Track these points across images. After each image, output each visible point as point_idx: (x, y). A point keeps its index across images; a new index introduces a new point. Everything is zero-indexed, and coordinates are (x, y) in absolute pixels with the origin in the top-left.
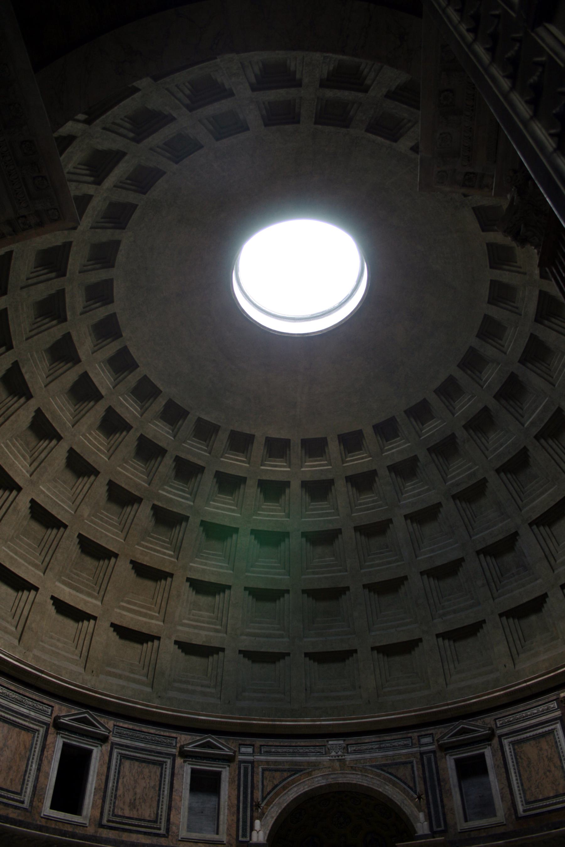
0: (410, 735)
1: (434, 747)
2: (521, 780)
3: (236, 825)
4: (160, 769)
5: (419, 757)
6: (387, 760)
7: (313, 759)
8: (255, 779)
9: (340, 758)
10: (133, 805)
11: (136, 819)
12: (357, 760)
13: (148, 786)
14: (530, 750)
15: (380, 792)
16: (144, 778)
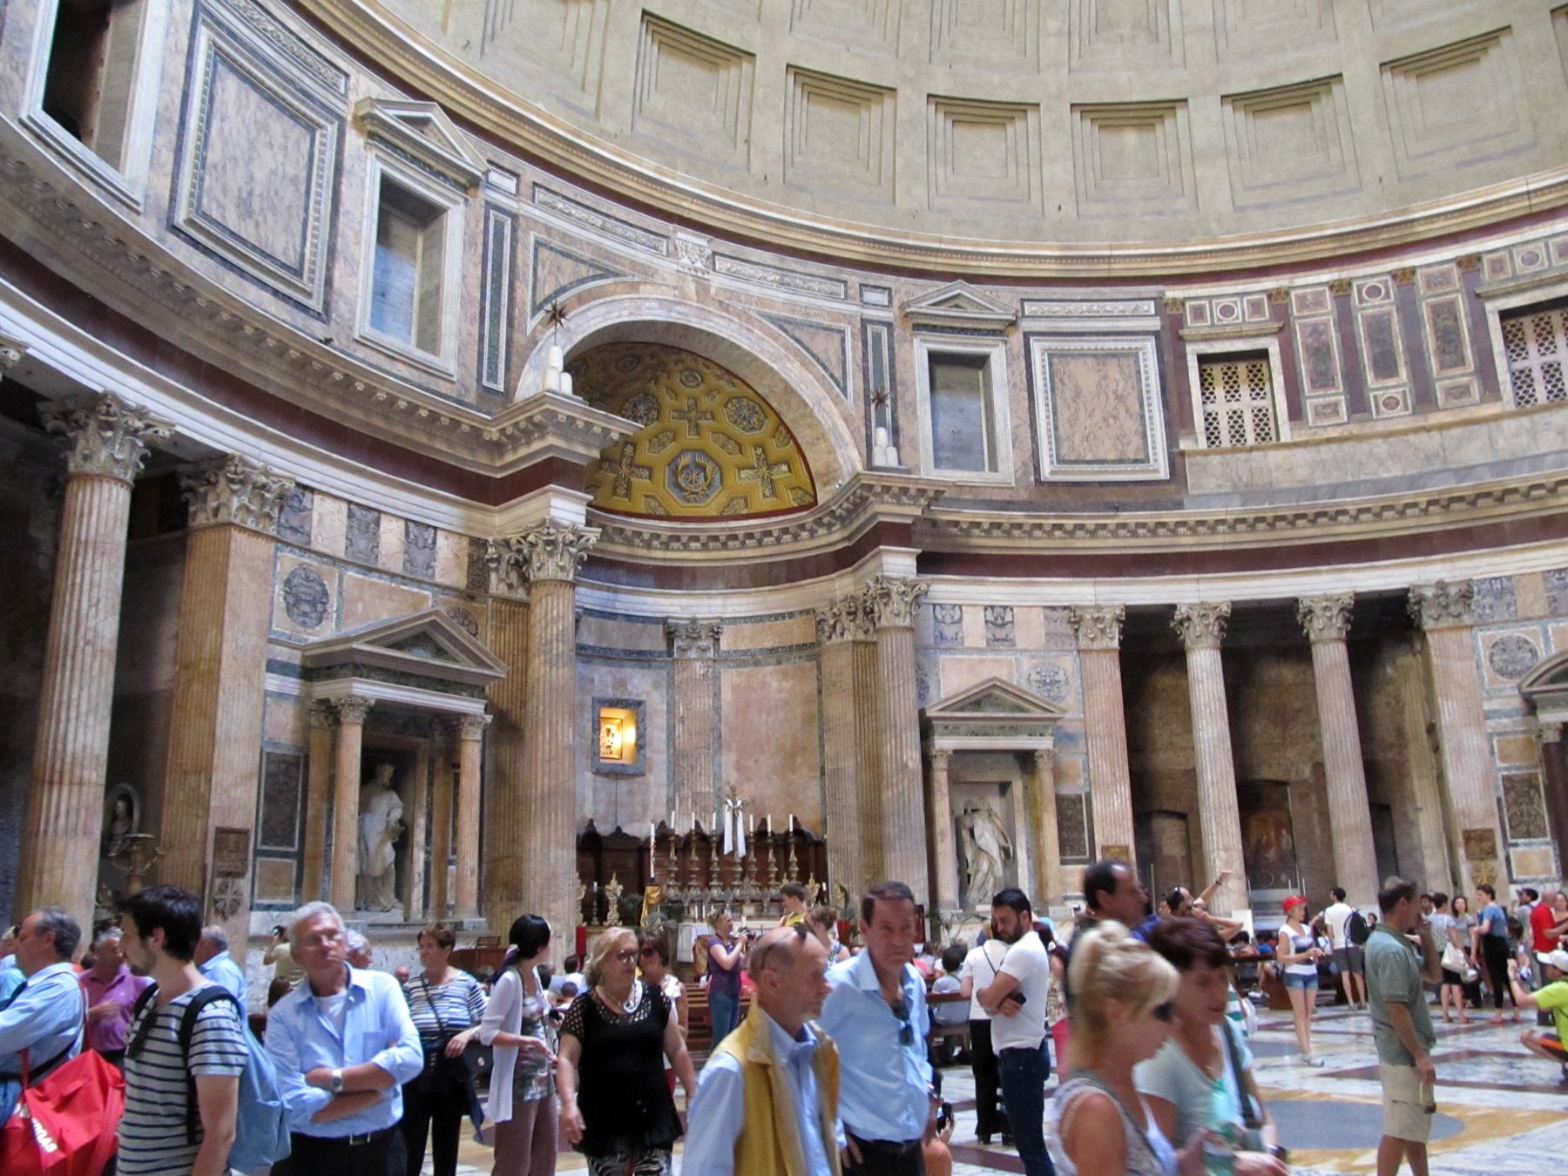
0: (844, 276)
1: (891, 315)
2: (1055, 420)
3: (476, 348)
4: (308, 139)
5: (859, 325)
6: (793, 311)
7: (642, 256)
8: (520, 256)
9: (700, 274)
10: (245, 206)
11: (254, 248)
12: (732, 292)
13: (280, 171)
14: (1083, 374)
15: (772, 369)
16: (271, 146)
